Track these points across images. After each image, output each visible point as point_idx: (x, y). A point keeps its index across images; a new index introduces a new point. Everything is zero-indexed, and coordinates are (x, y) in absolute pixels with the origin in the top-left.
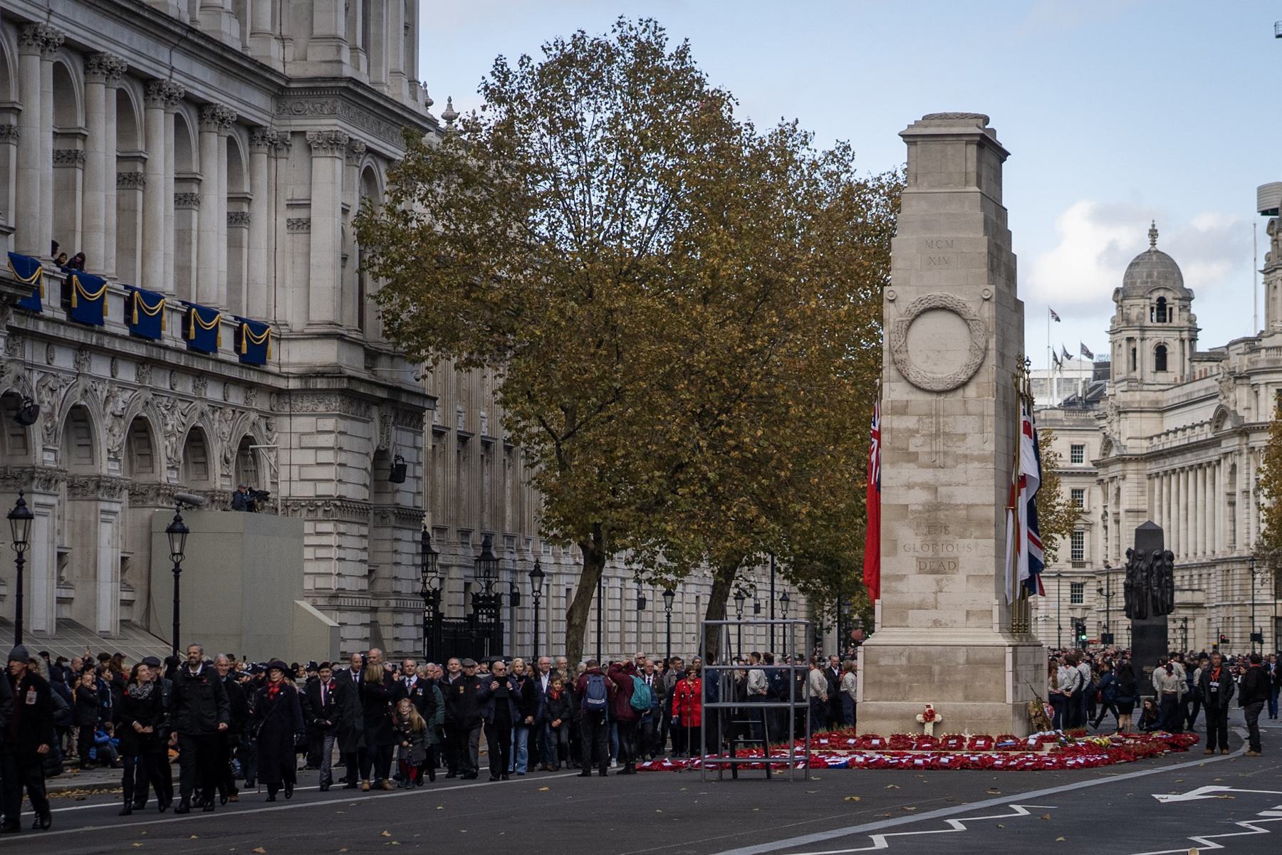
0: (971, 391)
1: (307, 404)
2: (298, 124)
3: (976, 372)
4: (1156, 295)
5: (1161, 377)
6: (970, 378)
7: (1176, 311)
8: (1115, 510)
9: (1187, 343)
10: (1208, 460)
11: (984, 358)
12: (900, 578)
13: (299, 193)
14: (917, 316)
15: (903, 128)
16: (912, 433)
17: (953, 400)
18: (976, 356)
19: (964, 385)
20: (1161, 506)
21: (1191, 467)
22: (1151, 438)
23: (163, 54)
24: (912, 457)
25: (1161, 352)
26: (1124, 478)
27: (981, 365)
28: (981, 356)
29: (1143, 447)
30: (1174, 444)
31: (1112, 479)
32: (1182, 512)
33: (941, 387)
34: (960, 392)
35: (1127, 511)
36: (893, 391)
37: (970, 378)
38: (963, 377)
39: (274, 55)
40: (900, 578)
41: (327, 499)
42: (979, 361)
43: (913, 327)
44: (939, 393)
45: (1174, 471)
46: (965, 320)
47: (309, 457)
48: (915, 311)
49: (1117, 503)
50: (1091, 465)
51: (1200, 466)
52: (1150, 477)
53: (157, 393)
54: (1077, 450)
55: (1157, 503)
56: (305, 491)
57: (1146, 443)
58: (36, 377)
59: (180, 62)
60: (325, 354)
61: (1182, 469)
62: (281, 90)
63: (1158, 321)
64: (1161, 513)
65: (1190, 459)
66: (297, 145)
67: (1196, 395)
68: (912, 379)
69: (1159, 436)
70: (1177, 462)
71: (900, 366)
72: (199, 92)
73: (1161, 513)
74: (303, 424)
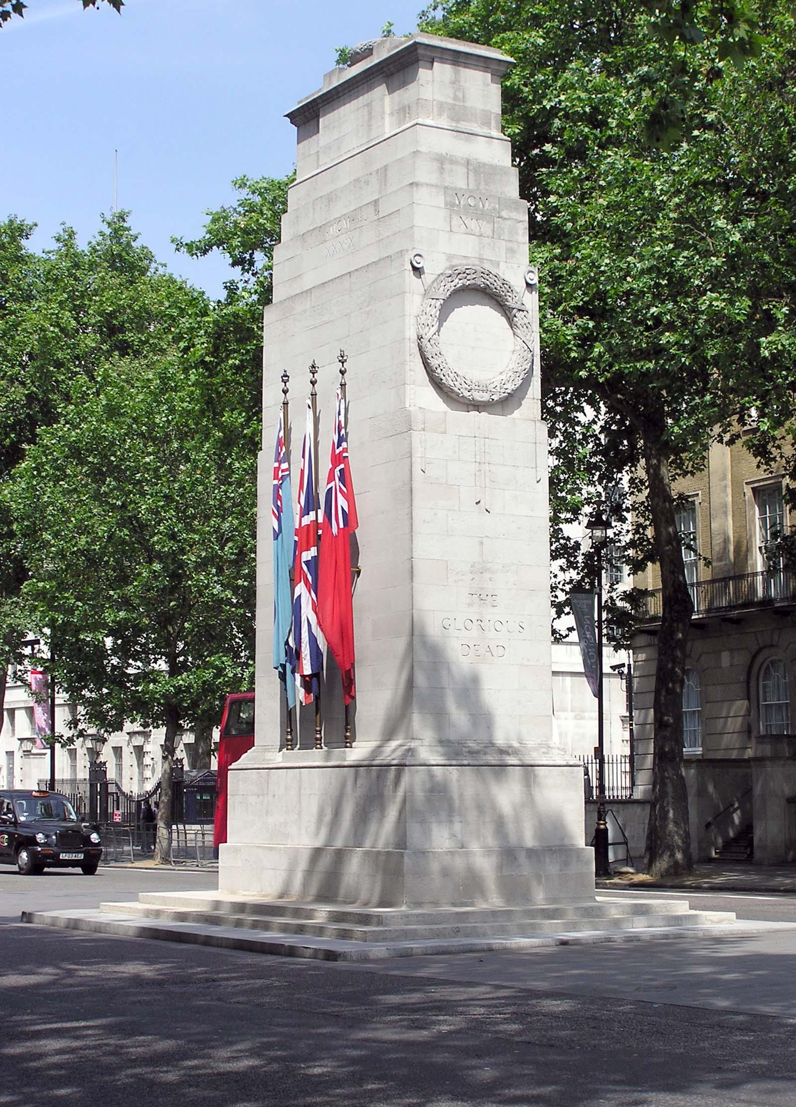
33: (485, 397)
68: (448, 381)
71: (434, 363)
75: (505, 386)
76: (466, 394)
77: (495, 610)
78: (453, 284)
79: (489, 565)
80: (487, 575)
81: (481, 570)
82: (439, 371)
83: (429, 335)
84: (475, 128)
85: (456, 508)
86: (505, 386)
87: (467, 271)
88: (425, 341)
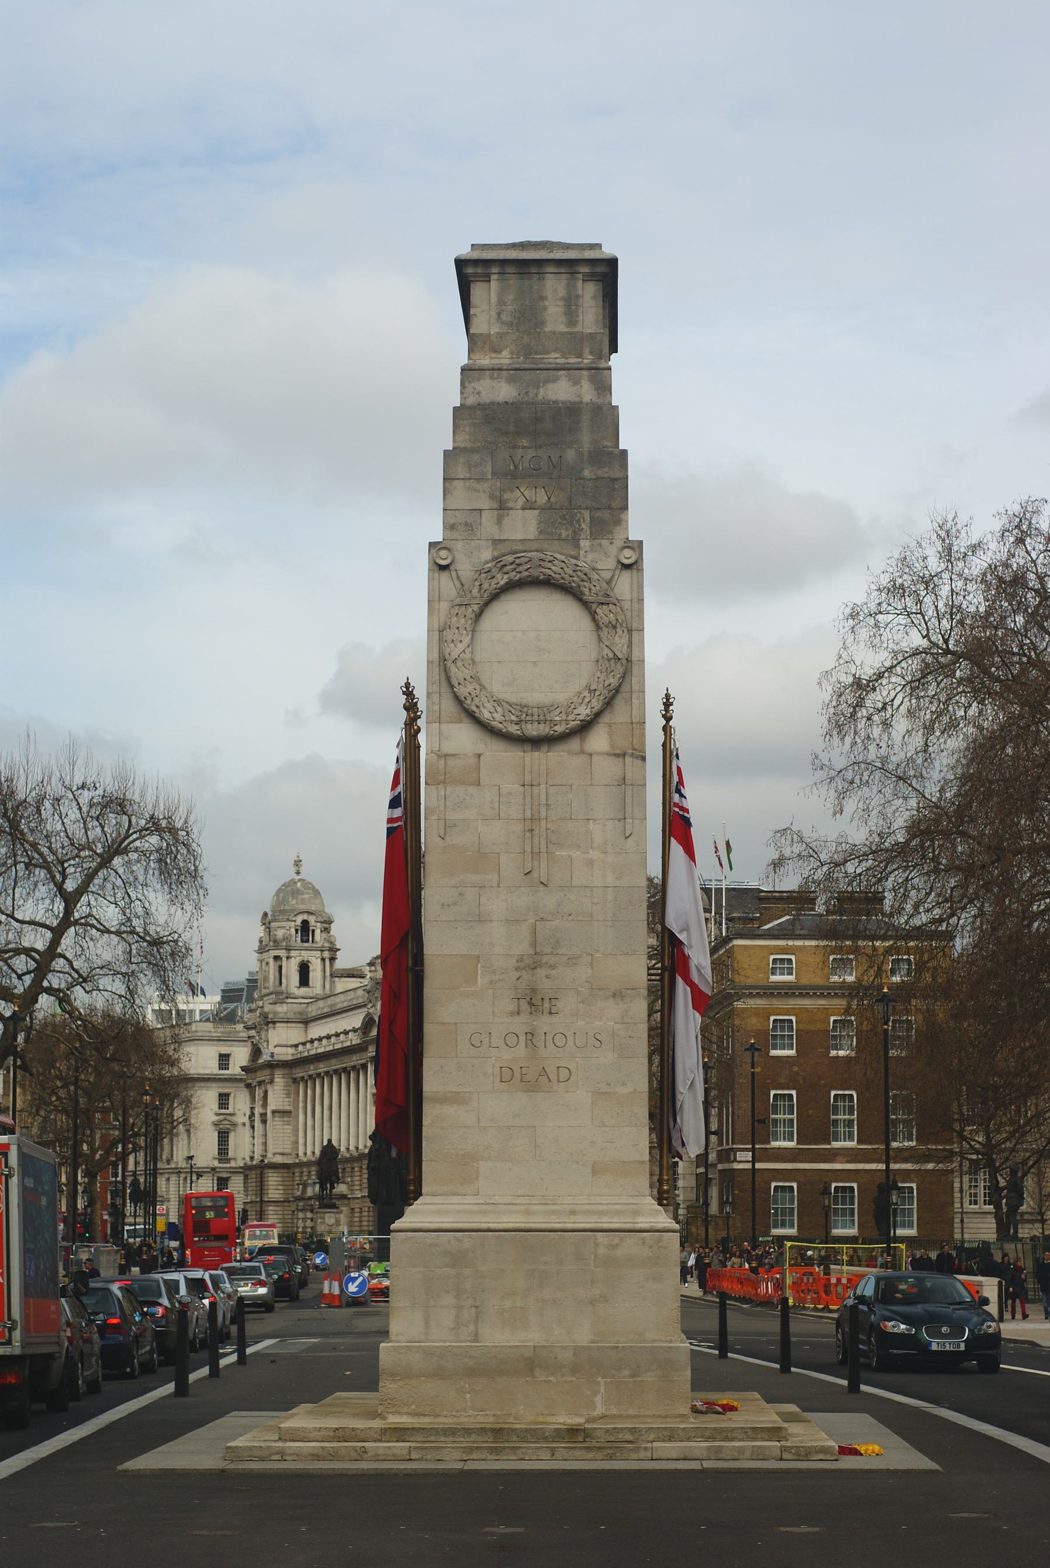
0: (598, 740)
3: (608, 703)
4: (299, 919)
5: (304, 991)
6: (598, 715)
7: (318, 932)
8: (262, 1111)
9: (327, 962)
10: (352, 1064)
11: (623, 677)
14: (495, 596)
15: (464, 251)
18: (609, 672)
19: (585, 727)
20: (305, 1107)
21: (336, 1071)
22: (296, 1046)
25: (304, 969)
26: (272, 1082)
27: (617, 690)
28: (620, 669)
29: (286, 1054)
30: (319, 1051)
31: (260, 1083)
32: (326, 1112)
33: (542, 730)
34: (574, 744)
35: (274, 1112)
37: (598, 715)
38: (584, 712)
42: (613, 681)
43: (486, 622)
44: (537, 742)
45: (319, 1075)
46: (586, 605)
48: (490, 586)
49: (265, 1105)
50: (238, 1071)
51: (345, 1069)
52: (295, 1081)
54: (224, 1060)
55: (301, 1105)
57: (291, 1051)
61: (327, 1073)
63: (302, 941)
64: (305, 1113)
65: (335, 1064)
67: (338, 1006)
69: (304, 1044)
70: (322, 1068)
71: (462, 692)
73: (305, 1113)
75: (576, 712)
76: (513, 729)
77: (555, 1019)
78: (494, 581)
79: (545, 959)
80: (542, 972)
81: (533, 963)
82: (469, 701)
83: (455, 654)
84: (554, 358)
85: (495, 884)
86: (576, 712)
87: (517, 561)
88: (449, 664)
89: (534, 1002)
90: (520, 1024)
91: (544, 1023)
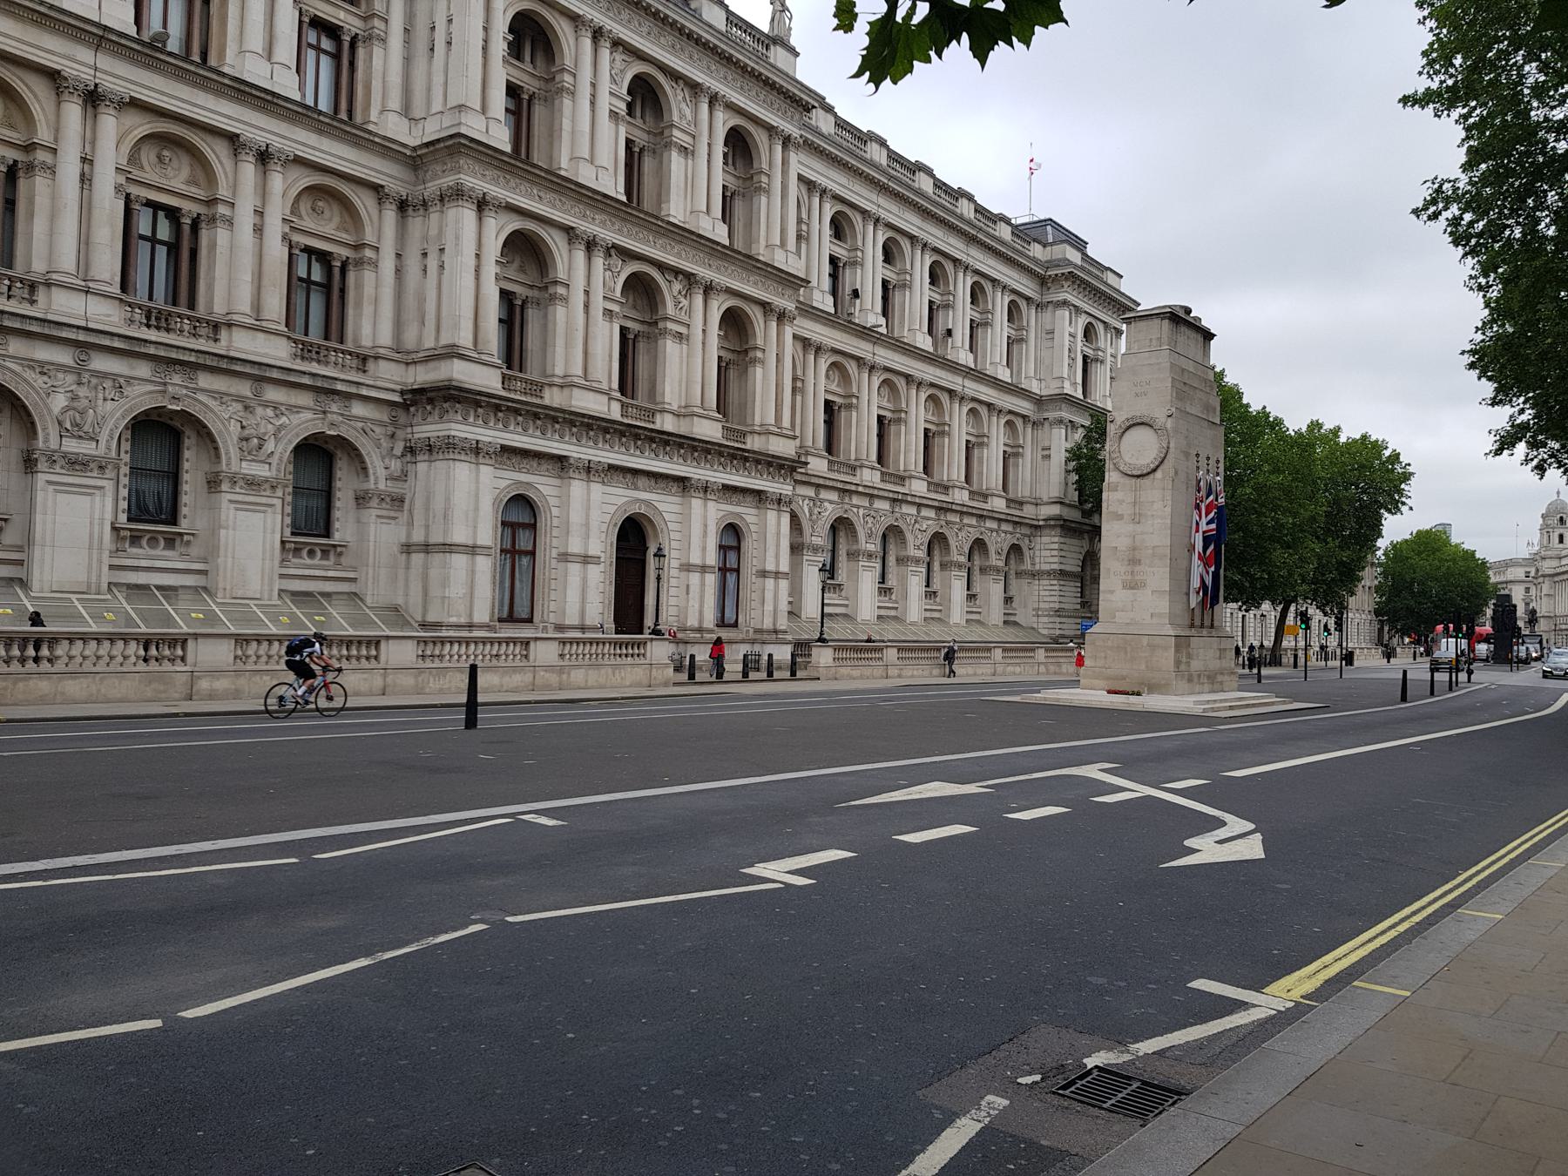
0: (1159, 474)
1: (1047, 531)
2: (1046, 415)
12: (1112, 592)
13: (1046, 444)
16: (1121, 502)
17: (1146, 482)
19: (1154, 470)
23: (959, 380)
24: (1119, 517)
36: (1111, 477)
39: (1035, 387)
40: (1112, 592)
41: (1054, 571)
47: (1048, 553)
53: (948, 523)
56: (1046, 567)
58: (861, 512)
59: (968, 383)
60: (1055, 510)
62: (1039, 401)
66: (1047, 424)
72: (983, 398)
74: (1045, 539)
89: (1134, 561)
90: (1129, 568)
91: (1137, 568)
